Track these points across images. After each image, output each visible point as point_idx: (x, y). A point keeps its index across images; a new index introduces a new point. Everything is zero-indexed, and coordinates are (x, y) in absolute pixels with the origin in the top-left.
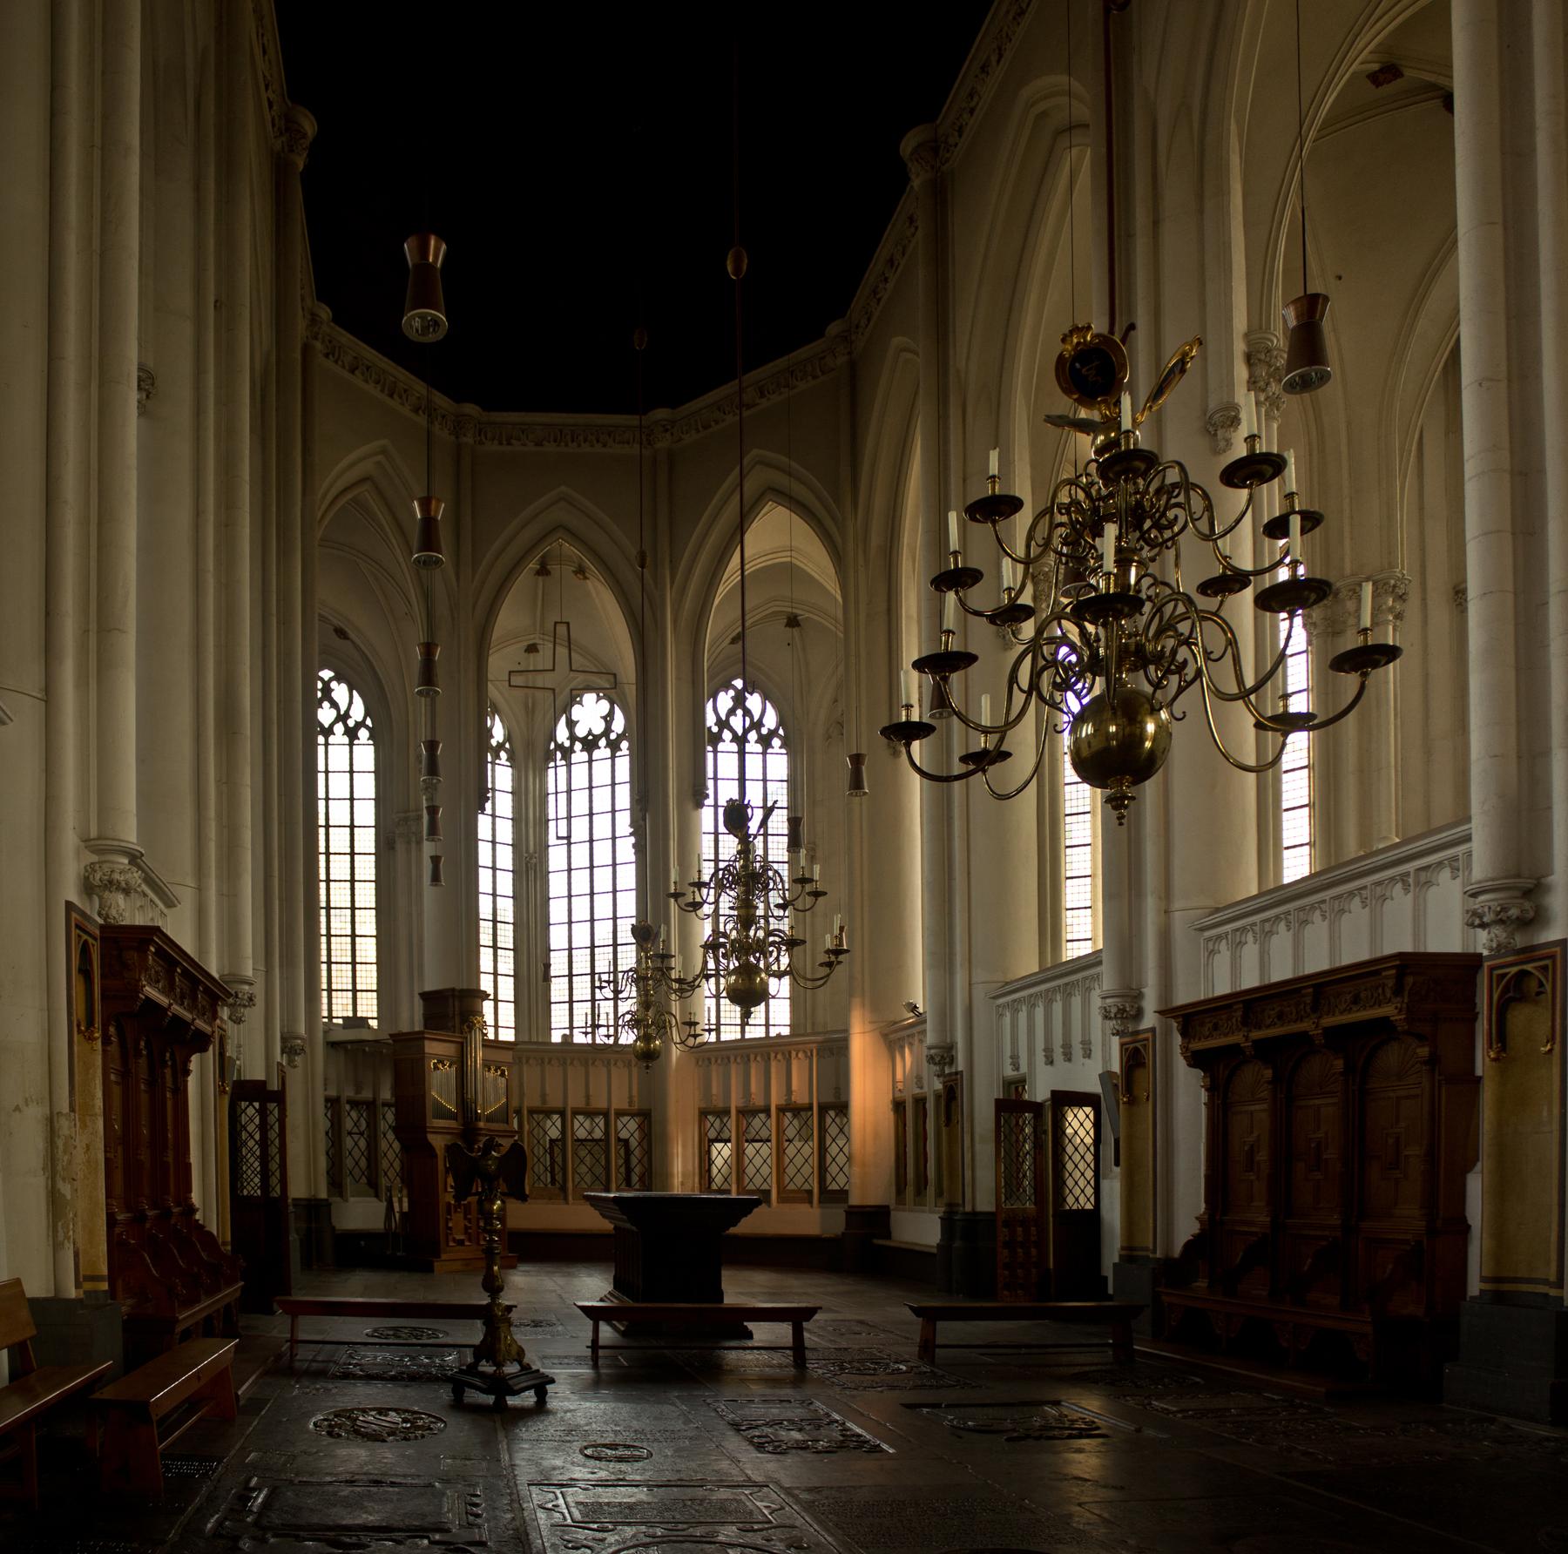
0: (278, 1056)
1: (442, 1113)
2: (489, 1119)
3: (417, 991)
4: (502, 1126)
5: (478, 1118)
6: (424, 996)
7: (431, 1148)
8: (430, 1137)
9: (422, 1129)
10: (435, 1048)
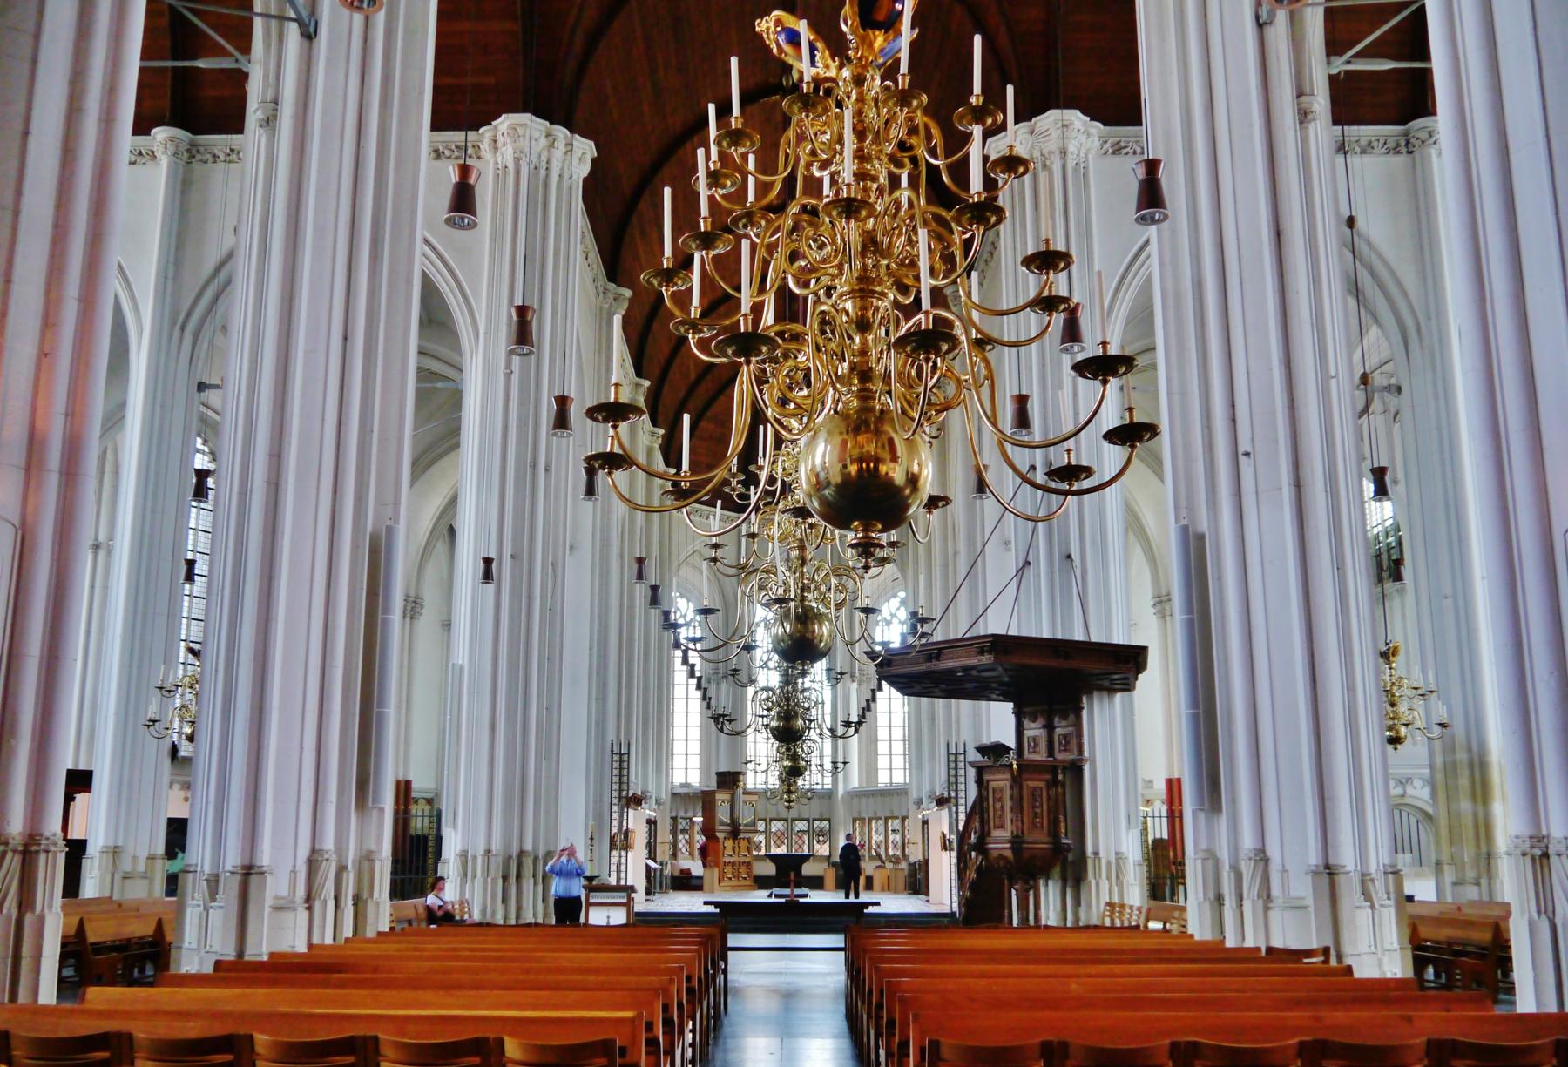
1: (723, 824)
2: (746, 825)
3: (714, 771)
4: (752, 828)
5: (740, 825)
6: (719, 774)
7: (717, 838)
8: (718, 834)
9: (714, 830)
10: (722, 797)
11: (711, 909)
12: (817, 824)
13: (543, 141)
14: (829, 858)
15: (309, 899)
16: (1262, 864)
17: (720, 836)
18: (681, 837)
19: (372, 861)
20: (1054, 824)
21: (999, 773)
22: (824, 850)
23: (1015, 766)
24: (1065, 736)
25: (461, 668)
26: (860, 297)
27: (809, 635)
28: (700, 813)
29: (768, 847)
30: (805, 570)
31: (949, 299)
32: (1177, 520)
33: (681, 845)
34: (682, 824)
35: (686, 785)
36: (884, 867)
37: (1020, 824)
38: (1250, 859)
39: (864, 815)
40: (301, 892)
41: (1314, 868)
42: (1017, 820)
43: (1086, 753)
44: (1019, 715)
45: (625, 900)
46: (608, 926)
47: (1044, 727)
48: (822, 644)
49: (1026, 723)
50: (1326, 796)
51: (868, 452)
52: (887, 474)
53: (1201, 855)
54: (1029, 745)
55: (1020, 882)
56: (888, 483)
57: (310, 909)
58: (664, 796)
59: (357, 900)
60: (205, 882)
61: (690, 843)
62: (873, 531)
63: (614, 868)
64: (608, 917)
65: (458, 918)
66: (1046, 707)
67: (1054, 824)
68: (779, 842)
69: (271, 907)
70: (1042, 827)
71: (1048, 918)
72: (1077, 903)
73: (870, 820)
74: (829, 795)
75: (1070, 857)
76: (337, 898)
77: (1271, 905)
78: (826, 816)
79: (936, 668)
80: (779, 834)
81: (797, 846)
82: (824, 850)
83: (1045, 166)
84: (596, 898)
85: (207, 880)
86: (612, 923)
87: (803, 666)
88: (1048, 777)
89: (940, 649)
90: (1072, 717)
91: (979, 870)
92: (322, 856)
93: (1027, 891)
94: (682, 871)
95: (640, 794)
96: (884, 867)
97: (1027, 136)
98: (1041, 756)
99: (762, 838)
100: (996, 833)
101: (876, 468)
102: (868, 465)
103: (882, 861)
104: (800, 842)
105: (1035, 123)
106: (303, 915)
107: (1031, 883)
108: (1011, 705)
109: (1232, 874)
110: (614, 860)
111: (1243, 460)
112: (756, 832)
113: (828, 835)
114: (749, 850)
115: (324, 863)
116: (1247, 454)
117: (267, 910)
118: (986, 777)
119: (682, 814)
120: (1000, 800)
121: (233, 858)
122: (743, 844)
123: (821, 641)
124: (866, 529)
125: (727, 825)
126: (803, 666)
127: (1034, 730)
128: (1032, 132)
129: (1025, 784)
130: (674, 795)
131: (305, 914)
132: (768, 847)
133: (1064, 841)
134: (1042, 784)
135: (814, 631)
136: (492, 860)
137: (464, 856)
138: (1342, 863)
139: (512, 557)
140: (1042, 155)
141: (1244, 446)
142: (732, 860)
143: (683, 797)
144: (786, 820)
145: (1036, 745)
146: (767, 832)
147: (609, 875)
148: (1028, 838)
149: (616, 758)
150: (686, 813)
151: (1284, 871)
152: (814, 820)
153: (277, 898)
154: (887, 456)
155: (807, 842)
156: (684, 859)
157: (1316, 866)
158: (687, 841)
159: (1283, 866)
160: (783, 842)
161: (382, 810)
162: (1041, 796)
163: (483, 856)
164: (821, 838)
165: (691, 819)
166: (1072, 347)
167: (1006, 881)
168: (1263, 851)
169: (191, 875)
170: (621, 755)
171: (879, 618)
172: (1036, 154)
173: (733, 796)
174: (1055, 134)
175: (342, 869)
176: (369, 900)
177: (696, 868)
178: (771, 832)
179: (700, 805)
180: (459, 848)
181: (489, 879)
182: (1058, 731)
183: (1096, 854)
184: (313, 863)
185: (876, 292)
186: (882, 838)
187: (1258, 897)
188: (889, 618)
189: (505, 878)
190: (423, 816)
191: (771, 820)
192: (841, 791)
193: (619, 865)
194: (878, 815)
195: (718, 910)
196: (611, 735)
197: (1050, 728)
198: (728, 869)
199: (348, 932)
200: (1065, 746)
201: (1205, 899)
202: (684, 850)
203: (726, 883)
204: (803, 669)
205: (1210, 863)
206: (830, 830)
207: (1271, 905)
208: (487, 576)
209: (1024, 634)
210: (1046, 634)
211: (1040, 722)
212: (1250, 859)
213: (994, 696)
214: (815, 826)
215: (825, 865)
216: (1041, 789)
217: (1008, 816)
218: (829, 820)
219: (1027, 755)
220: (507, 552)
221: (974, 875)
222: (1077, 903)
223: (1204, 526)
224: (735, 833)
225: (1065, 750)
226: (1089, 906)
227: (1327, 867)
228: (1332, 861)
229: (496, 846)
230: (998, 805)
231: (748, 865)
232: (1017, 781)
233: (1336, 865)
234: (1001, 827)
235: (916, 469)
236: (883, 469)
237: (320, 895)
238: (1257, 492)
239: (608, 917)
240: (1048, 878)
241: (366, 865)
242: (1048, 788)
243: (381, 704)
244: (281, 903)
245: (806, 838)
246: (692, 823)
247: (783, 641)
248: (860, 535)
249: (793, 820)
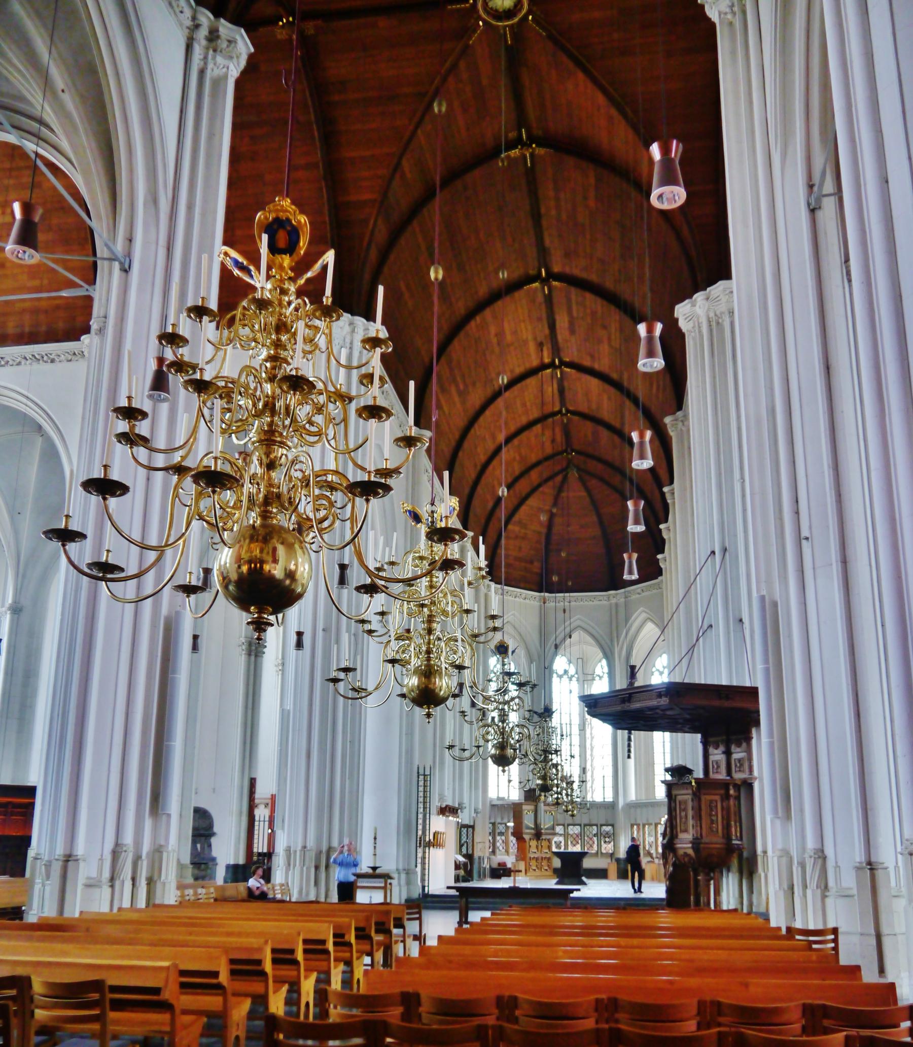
0: (473, 815)
1: (528, 828)
2: (546, 829)
5: (541, 829)
7: (524, 839)
8: (525, 836)
10: (528, 809)
11: (453, 892)
12: (604, 827)
13: (347, 329)
14: (612, 855)
15: (112, 879)
16: (820, 861)
17: (527, 837)
18: (498, 838)
19: (161, 852)
20: (727, 828)
21: (683, 789)
22: (608, 848)
23: (693, 784)
24: (739, 760)
25: (289, 711)
26: (266, 445)
27: (431, 686)
28: (512, 820)
29: (566, 846)
30: (432, 638)
31: (668, 426)
32: (757, 591)
33: (498, 844)
34: (501, 828)
35: (499, 799)
36: (653, 862)
37: (699, 828)
38: (811, 857)
39: (638, 822)
40: (106, 874)
41: (858, 865)
42: (697, 826)
43: (756, 773)
44: (706, 744)
45: (383, 885)
46: (371, 904)
47: (724, 753)
48: (442, 693)
49: (711, 750)
50: (868, 807)
51: (256, 556)
52: (270, 571)
53: (778, 853)
54: (713, 767)
55: (701, 874)
56: (271, 578)
57: (112, 886)
58: (480, 807)
59: (150, 882)
60: (43, 867)
61: (506, 842)
62: (265, 613)
63: (419, 861)
64: (371, 897)
65: (271, 896)
66: (724, 737)
67: (727, 828)
68: (574, 842)
69: (83, 885)
70: (717, 831)
71: (729, 903)
72: (751, 891)
73: (644, 826)
74: (611, 807)
75: (745, 854)
76: (134, 879)
77: (827, 894)
78: (610, 822)
79: (628, 708)
80: (575, 836)
81: (589, 846)
82: (608, 848)
83: (718, 323)
84: (361, 883)
85: (45, 865)
86: (374, 901)
87: (429, 709)
88: (722, 792)
89: (630, 694)
90: (744, 745)
91: (674, 865)
92: (122, 848)
93: (709, 881)
94: (499, 864)
95: (457, 806)
96: (653, 862)
97: (705, 302)
98: (722, 776)
99: (561, 839)
100: (682, 836)
101: (261, 567)
102: (256, 565)
103: (652, 857)
104: (591, 842)
105: (710, 292)
106: (107, 891)
107: (712, 875)
108: (699, 736)
109: (800, 869)
110: (420, 855)
111: (804, 542)
112: (555, 834)
113: (612, 837)
114: (549, 847)
115: (123, 853)
116: (807, 539)
117: (80, 887)
118: (674, 792)
119: (499, 820)
120: (685, 810)
121: (60, 851)
122: (545, 844)
123: (441, 690)
124: (260, 612)
125: (532, 829)
126: (429, 709)
127: (717, 755)
128: (707, 299)
129: (703, 798)
130: (493, 806)
131: (109, 890)
132: (566, 846)
133: (734, 842)
134: (717, 798)
135: (435, 683)
136: (307, 854)
137: (288, 850)
138: (881, 860)
139: (324, 630)
140: (716, 315)
141: (805, 533)
142: (536, 856)
143: (500, 808)
144: (580, 825)
145: (718, 767)
146: (566, 835)
147: (416, 866)
148: (705, 840)
149: (421, 777)
150: (502, 819)
151: (837, 867)
152: (602, 825)
153: (88, 878)
154: (270, 559)
155: (596, 842)
156: (501, 855)
157: (860, 863)
158: (503, 841)
159: (836, 862)
160: (578, 843)
161: (169, 815)
162: (716, 806)
163: (301, 851)
164: (607, 840)
165: (506, 824)
166: (642, 463)
167: (691, 873)
168: (822, 851)
169: (39, 861)
170: (424, 775)
171: (654, 669)
172: (712, 315)
173: (536, 807)
174: (724, 299)
175: (137, 859)
176: (158, 882)
177: (510, 861)
178: (568, 834)
179: (512, 815)
180: (285, 845)
181: (305, 868)
182: (735, 756)
183: (765, 852)
184: (116, 854)
185: (275, 441)
186: (652, 839)
187: (817, 887)
188: (661, 669)
189: (317, 868)
190: (264, 821)
191: (569, 825)
192: (621, 803)
193: (424, 858)
194: (650, 821)
195: (458, 893)
196: (416, 762)
197: (728, 753)
198: (533, 863)
199: (141, 903)
200: (740, 767)
201: (780, 888)
202: (501, 848)
203: (531, 873)
204: (429, 712)
205: (784, 860)
206: (613, 834)
207: (827, 894)
208: (299, 645)
209: (709, 682)
210: (724, 682)
211: (722, 748)
212: (811, 857)
213: (687, 729)
214: (602, 830)
215: (609, 860)
216: (716, 801)
217: (691, 822)
218: (613, 825)
219: (712, 776)
220: (320, 625)
221: (671, 869)
222: (751, 891)
223: (777, 597)
224: (538, 835)
225: (740, 771)
226: (760, 893)
227: (869, 863)
228: (873, 860)
229: (311, 843)
230: (683, 814)
231: (549, 859)
232: (697, 795)
233: (876, 862)
234: (686, 831)
235: (293, 567)
236: (267, 567)
237: (119, 877)
238: (814, 568)
239: (371, 897)
240: (728, 870)
241: (157, 855)
242: (722, 801)
243: (170, 739)
244: (91, 882)
245: (595, 839)
246: (507, 827)
247: (413, 691)
248: (256, 616)
249: (585, 825)
